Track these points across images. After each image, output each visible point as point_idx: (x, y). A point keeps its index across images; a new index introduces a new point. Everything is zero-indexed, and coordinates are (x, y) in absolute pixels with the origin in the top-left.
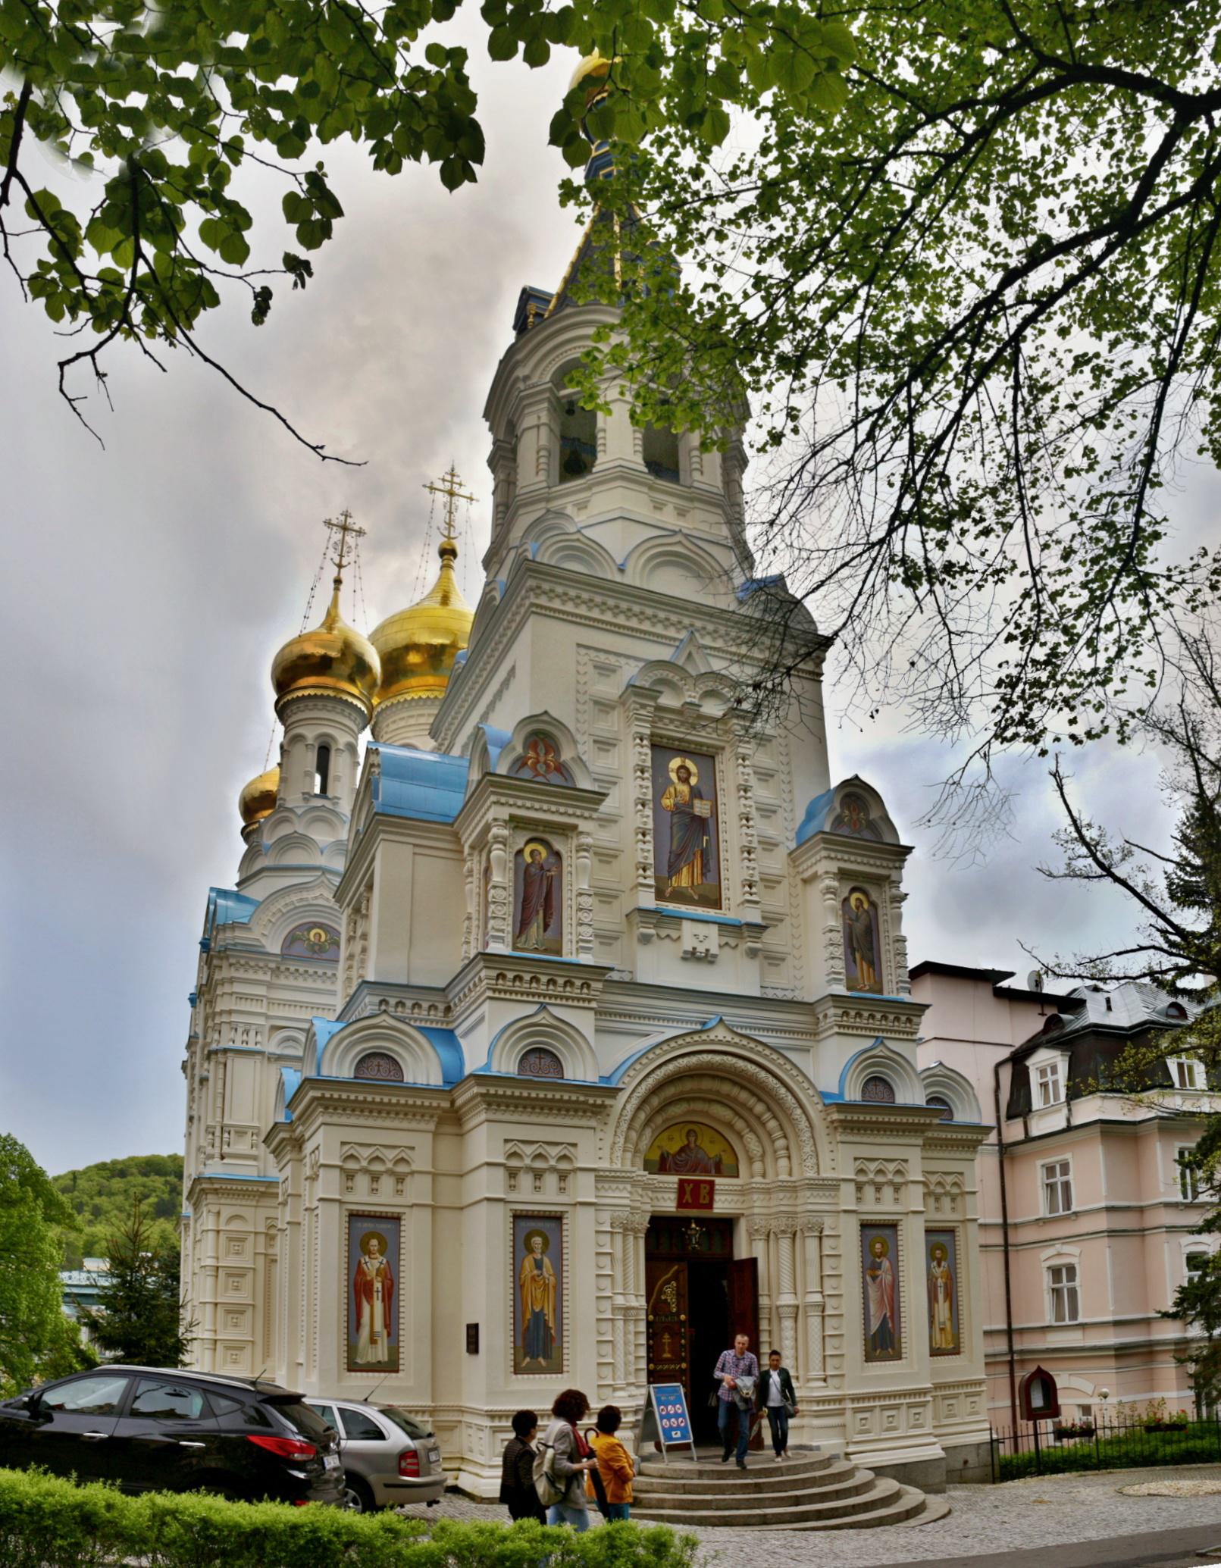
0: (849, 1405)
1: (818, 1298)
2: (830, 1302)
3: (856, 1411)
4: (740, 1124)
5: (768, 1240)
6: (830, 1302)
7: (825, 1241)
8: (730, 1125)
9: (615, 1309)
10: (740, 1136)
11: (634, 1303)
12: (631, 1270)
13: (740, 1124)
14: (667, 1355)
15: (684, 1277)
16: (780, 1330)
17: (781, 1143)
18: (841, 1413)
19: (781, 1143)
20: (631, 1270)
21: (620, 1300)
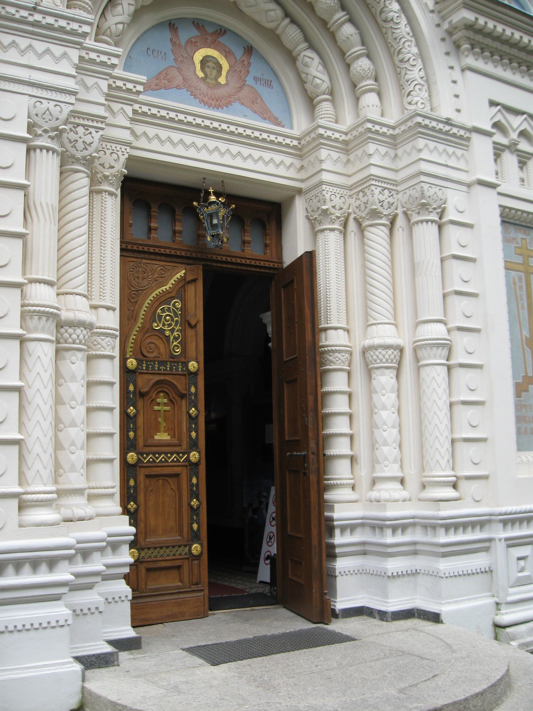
0: (501, 533)
1: (437, 331)
2: (461, 341)
3: (512, 543)
4: (291, 34)
5: (344, 232)
6: (461, 341)
7: (450, 230)
8: (274, 37)
9: (27, 314)
10: (292, 58)
11: (77, 309)
12: (78, 245)
13: (291, 34)
14: (163, 436)
15: (196, 296)
16: (371, 391)
17: (363, 65)
18: (485, 546)
19: (363, 65)
20: (78, 245)
21: (42, 295)
